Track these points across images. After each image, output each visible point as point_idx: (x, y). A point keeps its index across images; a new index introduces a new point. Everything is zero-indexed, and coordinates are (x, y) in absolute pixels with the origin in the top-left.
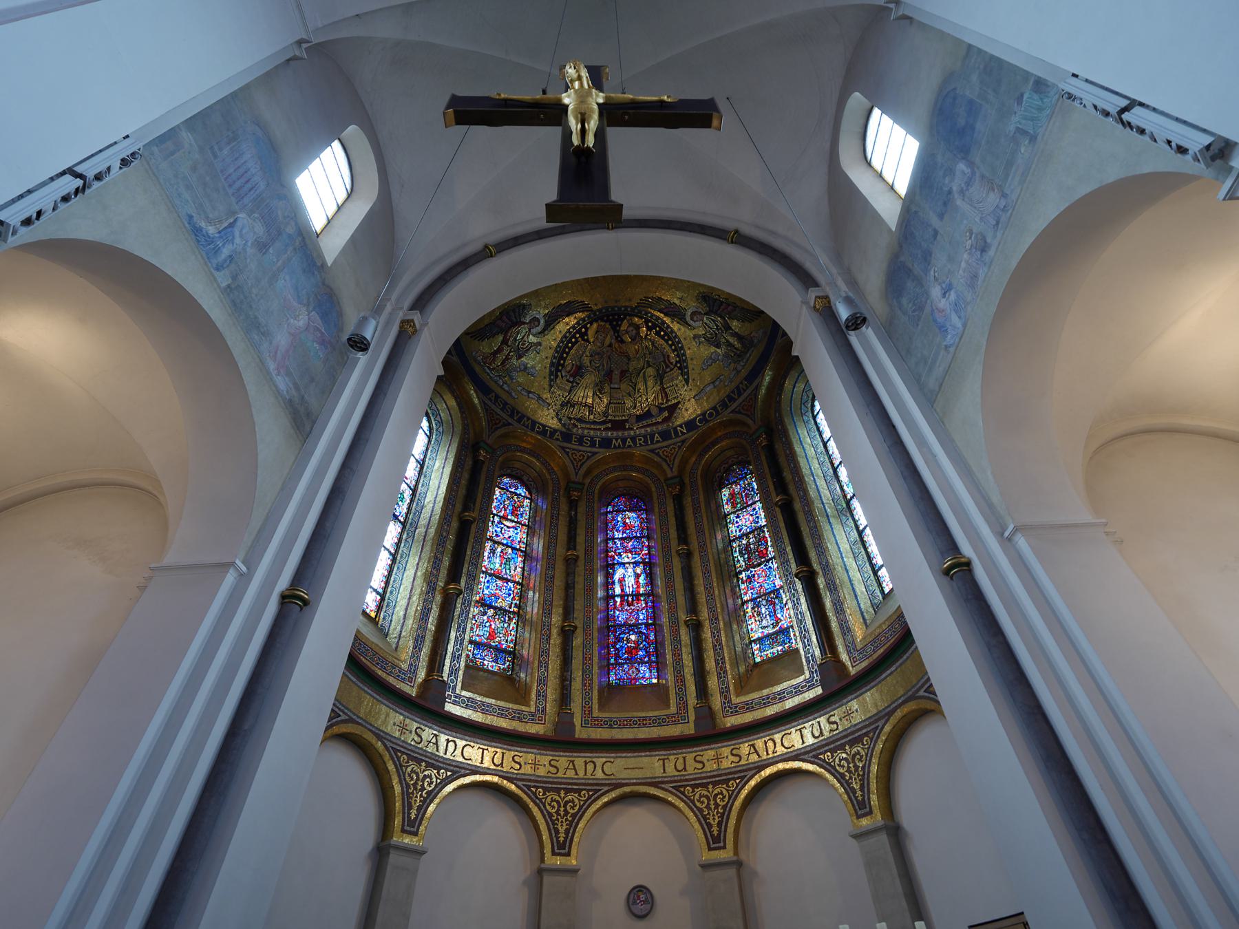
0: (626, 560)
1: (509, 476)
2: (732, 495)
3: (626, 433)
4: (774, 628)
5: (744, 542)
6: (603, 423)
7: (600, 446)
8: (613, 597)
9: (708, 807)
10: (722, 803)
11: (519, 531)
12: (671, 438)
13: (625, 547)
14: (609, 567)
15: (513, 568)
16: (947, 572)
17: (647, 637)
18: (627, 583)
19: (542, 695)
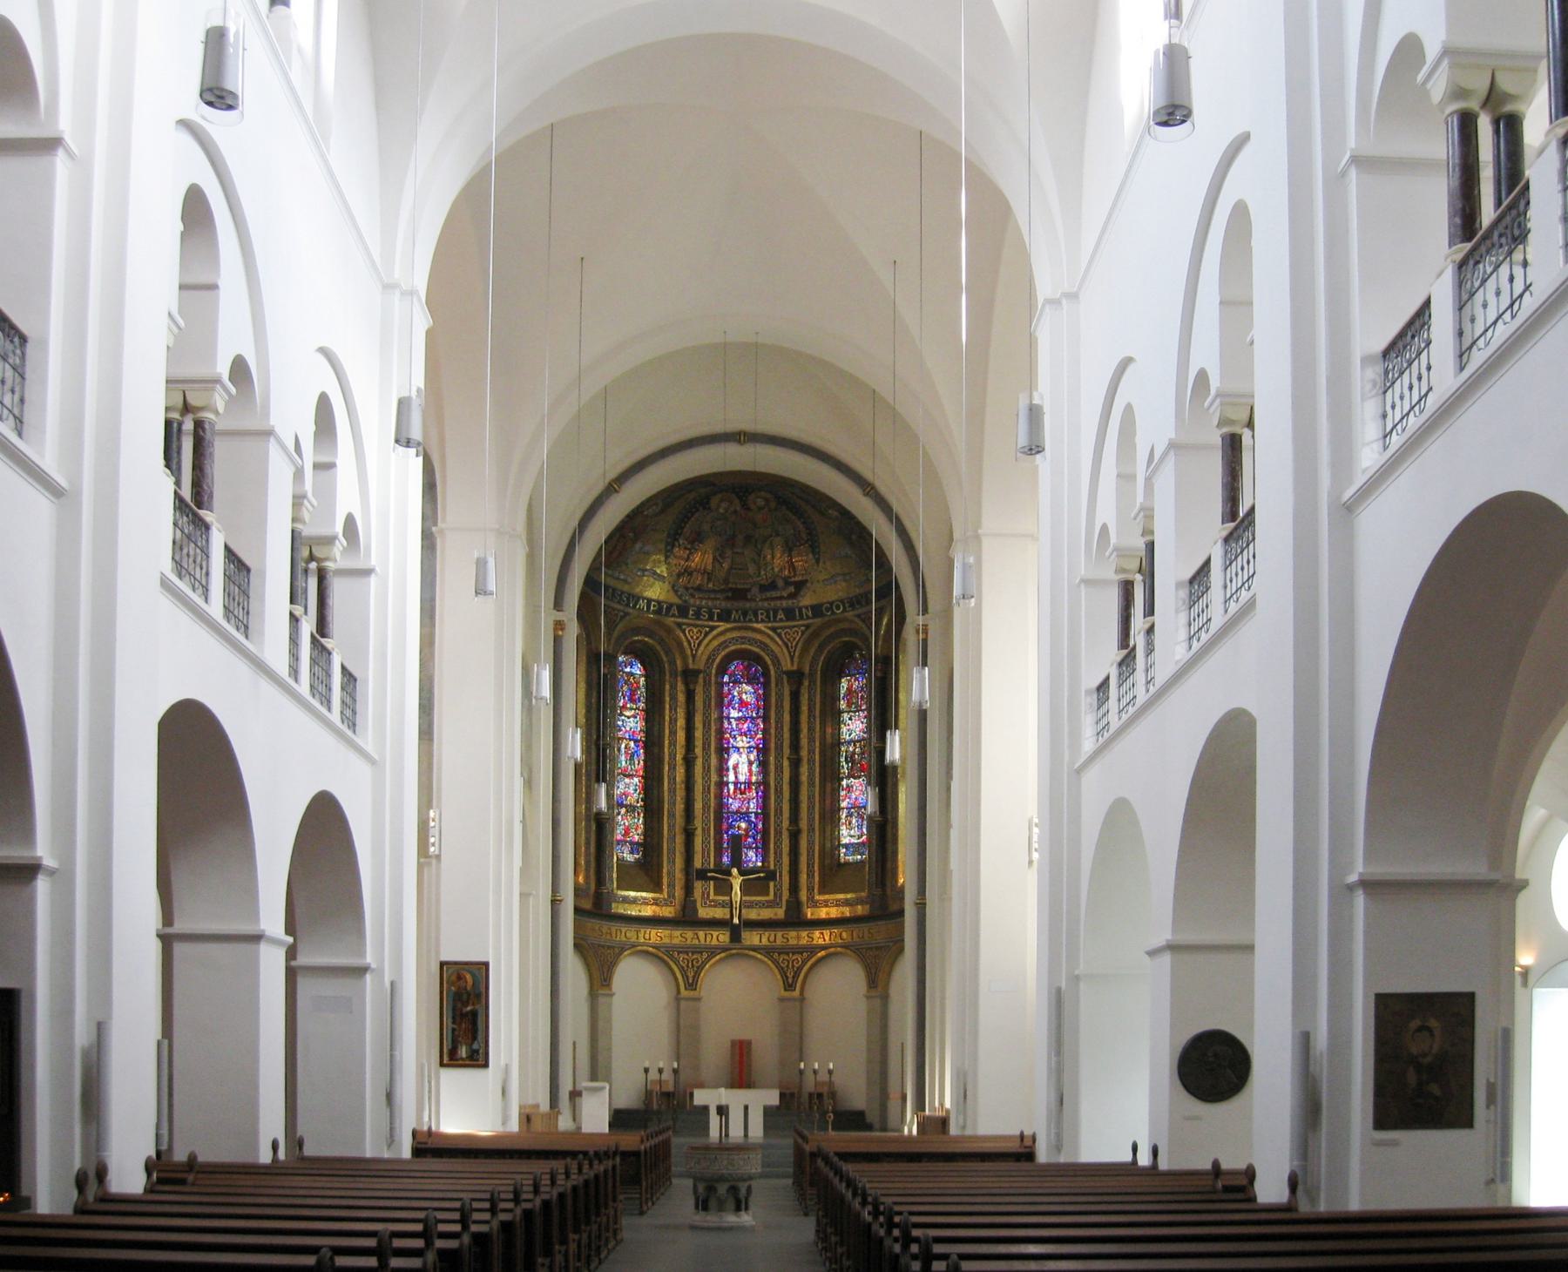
0: (740, 744)
1: (625, 653)
2: (849, 689)
3: (748, 605)
4: (858, 839)
5: (851, 749)
6: (722, 591)
7: (719, 620)
8: (727, 784)
9: (788, 966)
10: (797, 966)
11: (638, 719)
12: (794, 619)
13: (740, 729)
14: (723, 751)
15: (637, 762)
16: (917, 904)
17: (756, 825)
18: (740, 769)
19: (671, 885)
